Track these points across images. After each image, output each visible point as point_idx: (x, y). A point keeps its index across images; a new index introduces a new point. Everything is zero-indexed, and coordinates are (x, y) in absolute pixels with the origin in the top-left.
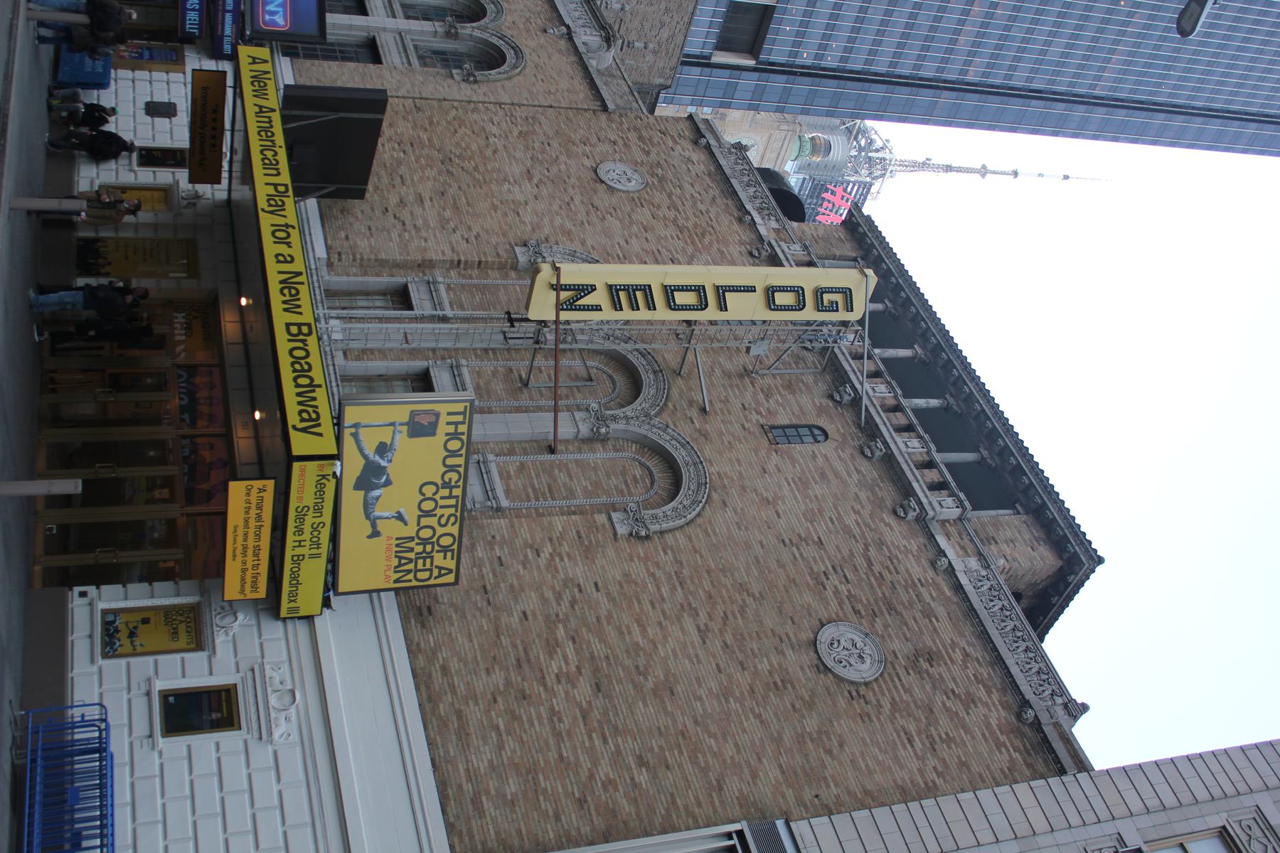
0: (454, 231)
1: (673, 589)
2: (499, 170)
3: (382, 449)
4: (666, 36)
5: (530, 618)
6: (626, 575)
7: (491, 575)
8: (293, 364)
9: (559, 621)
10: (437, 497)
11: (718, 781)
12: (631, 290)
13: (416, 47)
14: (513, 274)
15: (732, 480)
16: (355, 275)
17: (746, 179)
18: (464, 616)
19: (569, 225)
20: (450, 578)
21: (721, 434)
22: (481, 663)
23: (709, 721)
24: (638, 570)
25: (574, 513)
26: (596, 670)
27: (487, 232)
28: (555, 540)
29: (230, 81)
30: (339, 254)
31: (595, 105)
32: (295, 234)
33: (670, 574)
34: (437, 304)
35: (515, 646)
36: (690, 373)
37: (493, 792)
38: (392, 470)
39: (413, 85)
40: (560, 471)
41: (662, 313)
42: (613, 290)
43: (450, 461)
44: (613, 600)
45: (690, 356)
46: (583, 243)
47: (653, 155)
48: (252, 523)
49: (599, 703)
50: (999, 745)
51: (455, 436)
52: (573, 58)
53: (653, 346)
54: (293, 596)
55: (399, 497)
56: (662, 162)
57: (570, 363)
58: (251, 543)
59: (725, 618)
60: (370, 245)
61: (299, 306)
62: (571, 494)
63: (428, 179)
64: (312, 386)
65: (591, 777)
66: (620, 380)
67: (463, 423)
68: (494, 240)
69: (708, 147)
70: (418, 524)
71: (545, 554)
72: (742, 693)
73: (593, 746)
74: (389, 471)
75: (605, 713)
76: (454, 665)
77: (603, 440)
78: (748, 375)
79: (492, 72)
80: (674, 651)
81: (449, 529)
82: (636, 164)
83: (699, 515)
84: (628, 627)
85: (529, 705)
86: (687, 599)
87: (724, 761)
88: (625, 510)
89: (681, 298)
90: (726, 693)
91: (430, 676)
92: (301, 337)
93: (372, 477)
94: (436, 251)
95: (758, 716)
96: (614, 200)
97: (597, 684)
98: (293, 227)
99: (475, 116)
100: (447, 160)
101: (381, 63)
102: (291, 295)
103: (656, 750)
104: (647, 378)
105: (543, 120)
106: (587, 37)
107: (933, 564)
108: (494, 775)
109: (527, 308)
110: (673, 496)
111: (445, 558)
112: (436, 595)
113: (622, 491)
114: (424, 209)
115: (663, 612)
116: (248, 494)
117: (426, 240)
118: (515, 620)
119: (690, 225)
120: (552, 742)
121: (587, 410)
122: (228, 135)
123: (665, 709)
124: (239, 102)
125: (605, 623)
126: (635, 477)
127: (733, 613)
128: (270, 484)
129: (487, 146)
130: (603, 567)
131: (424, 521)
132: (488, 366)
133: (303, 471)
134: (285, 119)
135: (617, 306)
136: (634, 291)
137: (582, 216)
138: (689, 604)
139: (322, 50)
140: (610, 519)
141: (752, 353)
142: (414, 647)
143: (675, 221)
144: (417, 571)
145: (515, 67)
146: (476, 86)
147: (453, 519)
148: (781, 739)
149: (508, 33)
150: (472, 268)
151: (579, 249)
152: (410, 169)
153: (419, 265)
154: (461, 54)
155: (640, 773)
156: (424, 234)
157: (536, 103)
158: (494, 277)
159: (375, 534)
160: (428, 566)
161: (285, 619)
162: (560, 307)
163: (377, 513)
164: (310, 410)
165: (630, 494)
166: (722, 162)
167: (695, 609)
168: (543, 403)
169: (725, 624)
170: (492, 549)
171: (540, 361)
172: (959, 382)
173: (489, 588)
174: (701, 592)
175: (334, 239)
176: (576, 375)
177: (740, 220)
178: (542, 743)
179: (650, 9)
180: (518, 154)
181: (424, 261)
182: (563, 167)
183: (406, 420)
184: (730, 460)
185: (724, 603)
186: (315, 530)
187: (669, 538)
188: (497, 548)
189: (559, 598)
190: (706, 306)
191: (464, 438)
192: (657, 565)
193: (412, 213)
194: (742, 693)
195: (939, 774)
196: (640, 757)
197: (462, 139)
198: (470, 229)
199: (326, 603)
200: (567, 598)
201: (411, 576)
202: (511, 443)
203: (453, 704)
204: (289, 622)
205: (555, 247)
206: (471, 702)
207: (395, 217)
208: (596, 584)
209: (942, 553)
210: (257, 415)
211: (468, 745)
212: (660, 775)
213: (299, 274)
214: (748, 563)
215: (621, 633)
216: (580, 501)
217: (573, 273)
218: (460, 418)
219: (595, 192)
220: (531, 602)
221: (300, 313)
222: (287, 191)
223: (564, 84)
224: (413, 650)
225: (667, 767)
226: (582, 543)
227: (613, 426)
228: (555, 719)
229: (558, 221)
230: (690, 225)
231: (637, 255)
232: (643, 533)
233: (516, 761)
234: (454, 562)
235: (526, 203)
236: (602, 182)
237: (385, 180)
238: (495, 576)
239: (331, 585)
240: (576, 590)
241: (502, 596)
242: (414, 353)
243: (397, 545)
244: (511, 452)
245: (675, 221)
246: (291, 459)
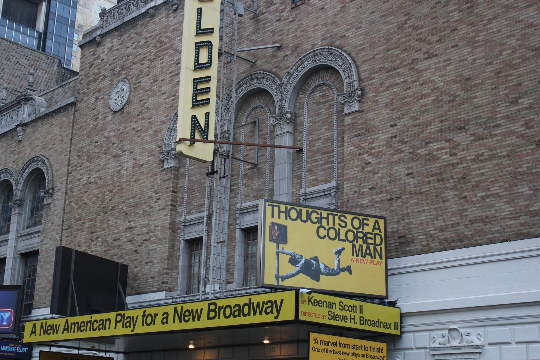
0: (152, 207)
1: (398, 75)
2: (112, 176)
3: (294, 261)
4: (25, 61)
5: (411, 171)
6: (387, 105)
7: (381, 195)
8: (235, 316)
9: (415, 152)
10: (327, 227)
11: (532, 51)
12: (196, 92)
13: (28, 227)
14: (182, 170)
15: (327, 31)
16: (177, 274)
17: (124, 11)
18: (407, 215)
19: (151, 132)
20: (381, 222)
21: (296, 37)
22: (440, 205)
23: (490, 55)
24: (384, 98)
25: (343, 138)
26: (450, 129)
27: (153, 186)
28: (360, 151)
29: (47, 349)
30: (163, 283)
31: (71, 110)
32: (149, 311)
33: (388, 76)
34: (199, 221)
35: (429, 182)
36: (254, 56)
37: (528, 203)
38: (308, 255)
39: (54, 230)
40: (314, 146)
41: (213, 72)
42: (196, 104)
43: (304, 218)
44: (403, 115)
45: (242, 55)
46: (163, 123)
47: (107, 73)
48: (337, 349)
49: (472, 128)
51: (287, 214)
52: (39, 123)
53: (234, 79)
54: (387, 325)
55: (325, 252)
56: (111, 67)
57: (243, 135)
58: (350, 350)
59: (420, 40)
60: (158, 263)
61: (197, 310)
62: (330, 139)
63: (116, 223)
64: (250, 304)
65: (522, 136)
66: (255, 103)
67: (279, 207)
68: (159, 182)
69: (102, 36)
70: (344, 241)
71: (369, 158)
72: (473, 31)
73: (501, 134)
74: (308, 258)
75: (479, 125)
76: (439, 223)
77: (295, 116)
78: (257, 16)
79: (47, 177)
80: (440, 76)
81: (349, 221)
82: (112, 85)
83: (349, 55)
84: (422, 106)
85: (470, 175)
86: (405, 66)
87: (519, 45)
88: (343, 104)
89: (203, 59)
90: (472, 42)
91: (445, 239)
92: (217, 310)
93: (311, 269)
94: (164, 220)
95: (490, 21)
96: (136, 100)
97: (459, 129)
98: (145, 311)
99: (76, 190)
100: (104, 210)
101: (38, 250)
102: (189, 315)
103: (507, 91)
104: (255, 85)
105: (80, 146)
106: (25, 113)
108: (516, 201)
109: (205, 162)
110: (336, 72)
111: (367, 225)
112: (392, 232)
113: (330, 106)
114: (136, 227)
115: (414, 82)
116: (318, 350)
117: (157, 226)
118: (412, 181)
119: (154, 50)
120: (496, 162)
121: (275, 126)
122: (81, 352)
123: (480, 84)
124: (60, 344)
125: (419, 121)
126: (321, 96)
127: (417, 35)
128: (312, 335)
129: (96, 183)
130: (380, 121)
131: (343, 237)
132: (242, 190)
133: (305, 314)
134: (73, 314)
135: (207, 102)
136: (197, 90)
137: (145, 123)
138: (409, 64)
139: (28, 289)
140: (348, 114)
141: (242, 13)
142: (426, 249)
143: (151, 61)
144: (375, 244)
145: (44, 162)
146: (56, 189)
147: (342, 218)
148: (507, 6)
149: (21, 166)
150: (177, 197)
151: (168, 125)
152: (109, 235)
153: (173, 231)
154: (34, 197)
155: (522, 103)
156: (153, 227)
157: (68, 149)
158: (184, 183)
159: (349, 269)
160: (372, 236)
161: (402, 332)
162: (205, 140)
163: (335, 267)
164: (265, 306)
165: (333, 100)
166: (112, 26)
167: (413, 60)
168: (268, 155)
169: (425, 41)
170: (363, 193)
171: (240, 155)
173: (389, 197)
174: (402, 56)
175: (153, 286)
176: (251, 132)
177: (152, 16)
178: (497, 168)
179: (7, 71)
180: (102, 163)
181: (170, 228)
182: (112, 134)
183: (275, 244)
184: (314, 31)
185: (410, 40)
186: (344, 308)
187: (364, 76)
188: (362, 191)
189: (399, 151)
190: (209, 42)
191: (289, 207)
192: (381, 84)
193: (138, 235)
194: (473, 31)
196: (511, 103)
197: (90, 199)
198: (150, 197)
199: (393, 304)
200: (399, 146)
201: (378, 248)
202: (294, 177)
203: (466, 226)
204: (403, 330)
205: (166, 142)
206: (465, 214)
207: (140, 246)
208: (391, 126)
210: (266, 342)
211: (494, 217)
212: (525, 90)
213: (176, 309)
214: (385, 23)
215: (425, 111)
216: (335, 133)
217: (183, 129)
218: (276, 209)
219: (129, 113)
220: (400, 170)
221: (202, 309)
222: (120, 315)
223: (56, 130)
224: (427, 250)
225: (520, 84)
226: (364, 134)
227: (286, 109)
228: (480, 158)
229: (147, 139)
230: (154, 50)
231: (174, 87)
232: (359, 93)
233: (507, 186)
234: (370, 219)
235: (134, 159)
236: (123, 108)
237: (116, 251)
238: (381, 193)
239: (380, 300)
240: (394, 139)
241: (396, 189)
242: (231, 238)
243: (357, 255)
244: (300, 177)
245: (151, 61)
246: (297, 321)
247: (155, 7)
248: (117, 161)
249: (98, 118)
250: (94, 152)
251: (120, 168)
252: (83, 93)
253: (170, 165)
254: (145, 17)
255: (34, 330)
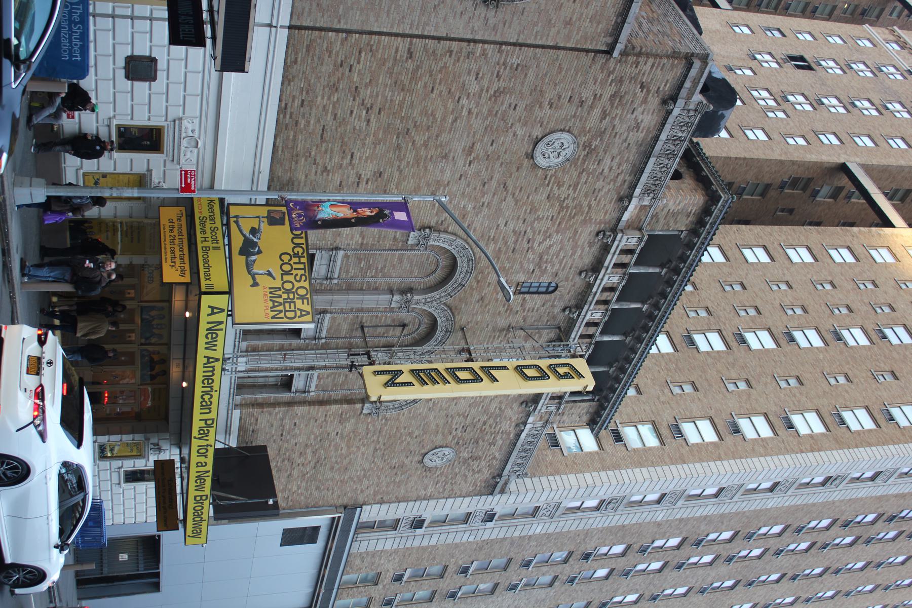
50: (475, 484)
69: (669, 113)
107: (517, 425)
119: (571, 205)
157: (540, 43)
172: (640, 340)
177: (621, 199)
195: (439, 492)
209: (525, 424)
220: (301, 439)
230: (571, 205)
231: (504, 237)
247: (626, 209)
248: (464, 151)
249: (550, 108)
250: (502, 104)
251: (451, 158)
252: (614, 69)
253: (410, 239)
254: (629, 188)
255: (215, 311)
